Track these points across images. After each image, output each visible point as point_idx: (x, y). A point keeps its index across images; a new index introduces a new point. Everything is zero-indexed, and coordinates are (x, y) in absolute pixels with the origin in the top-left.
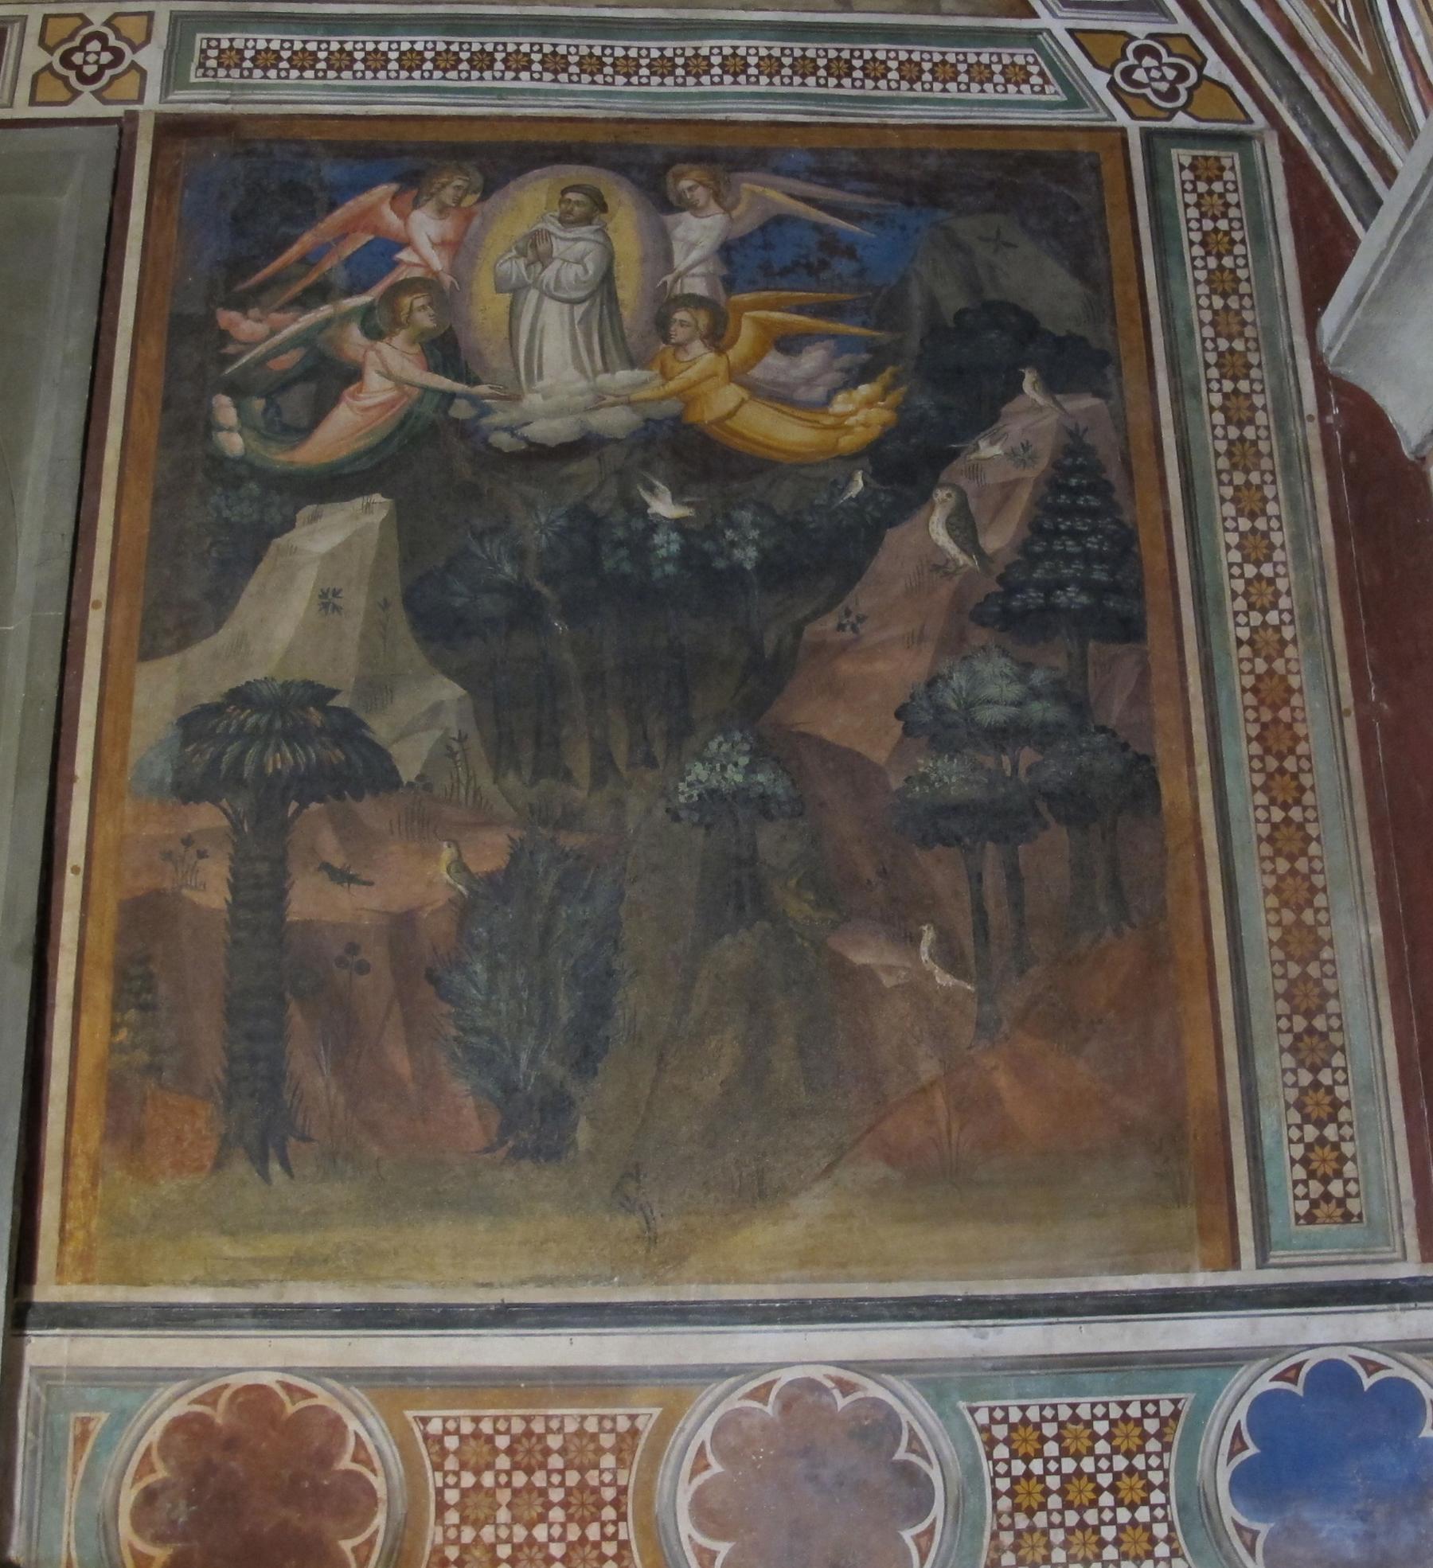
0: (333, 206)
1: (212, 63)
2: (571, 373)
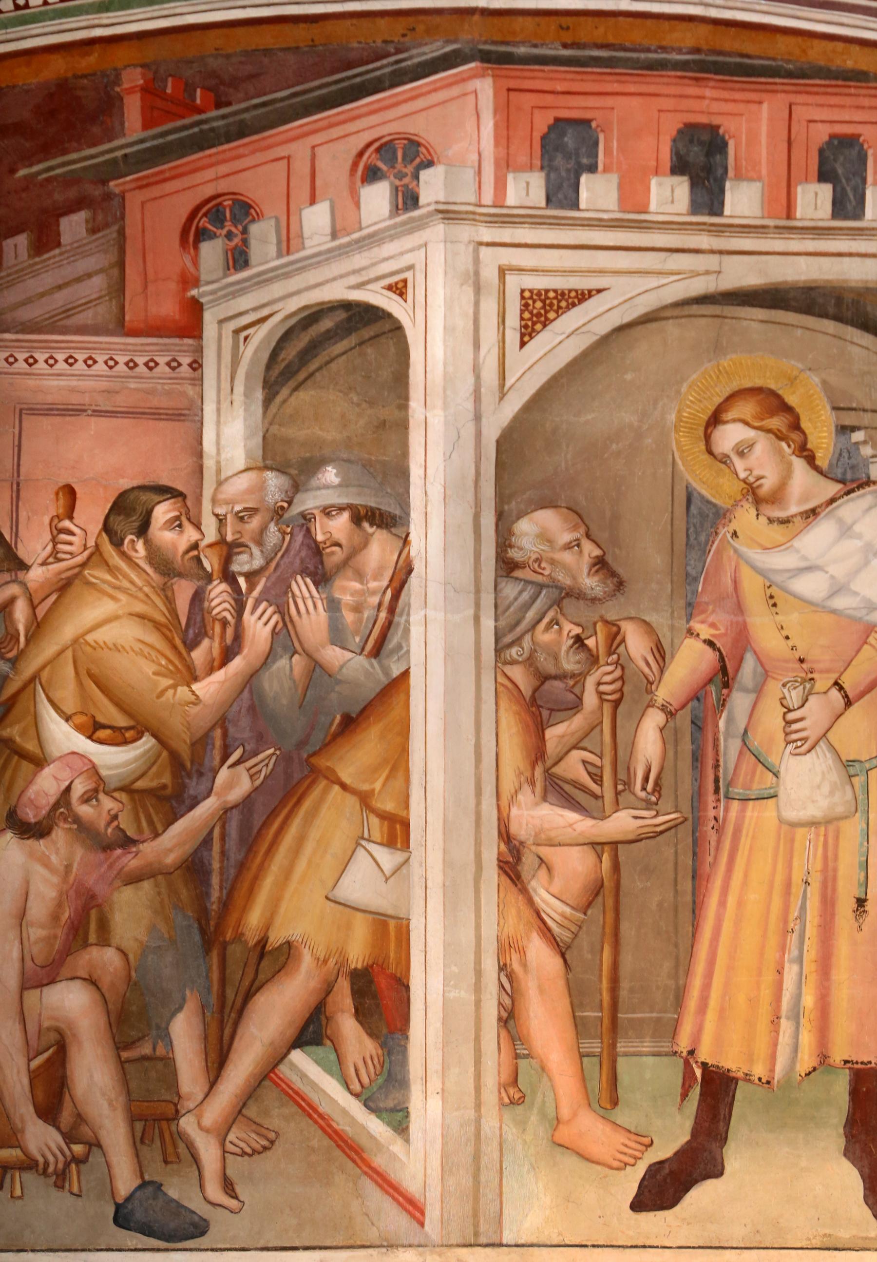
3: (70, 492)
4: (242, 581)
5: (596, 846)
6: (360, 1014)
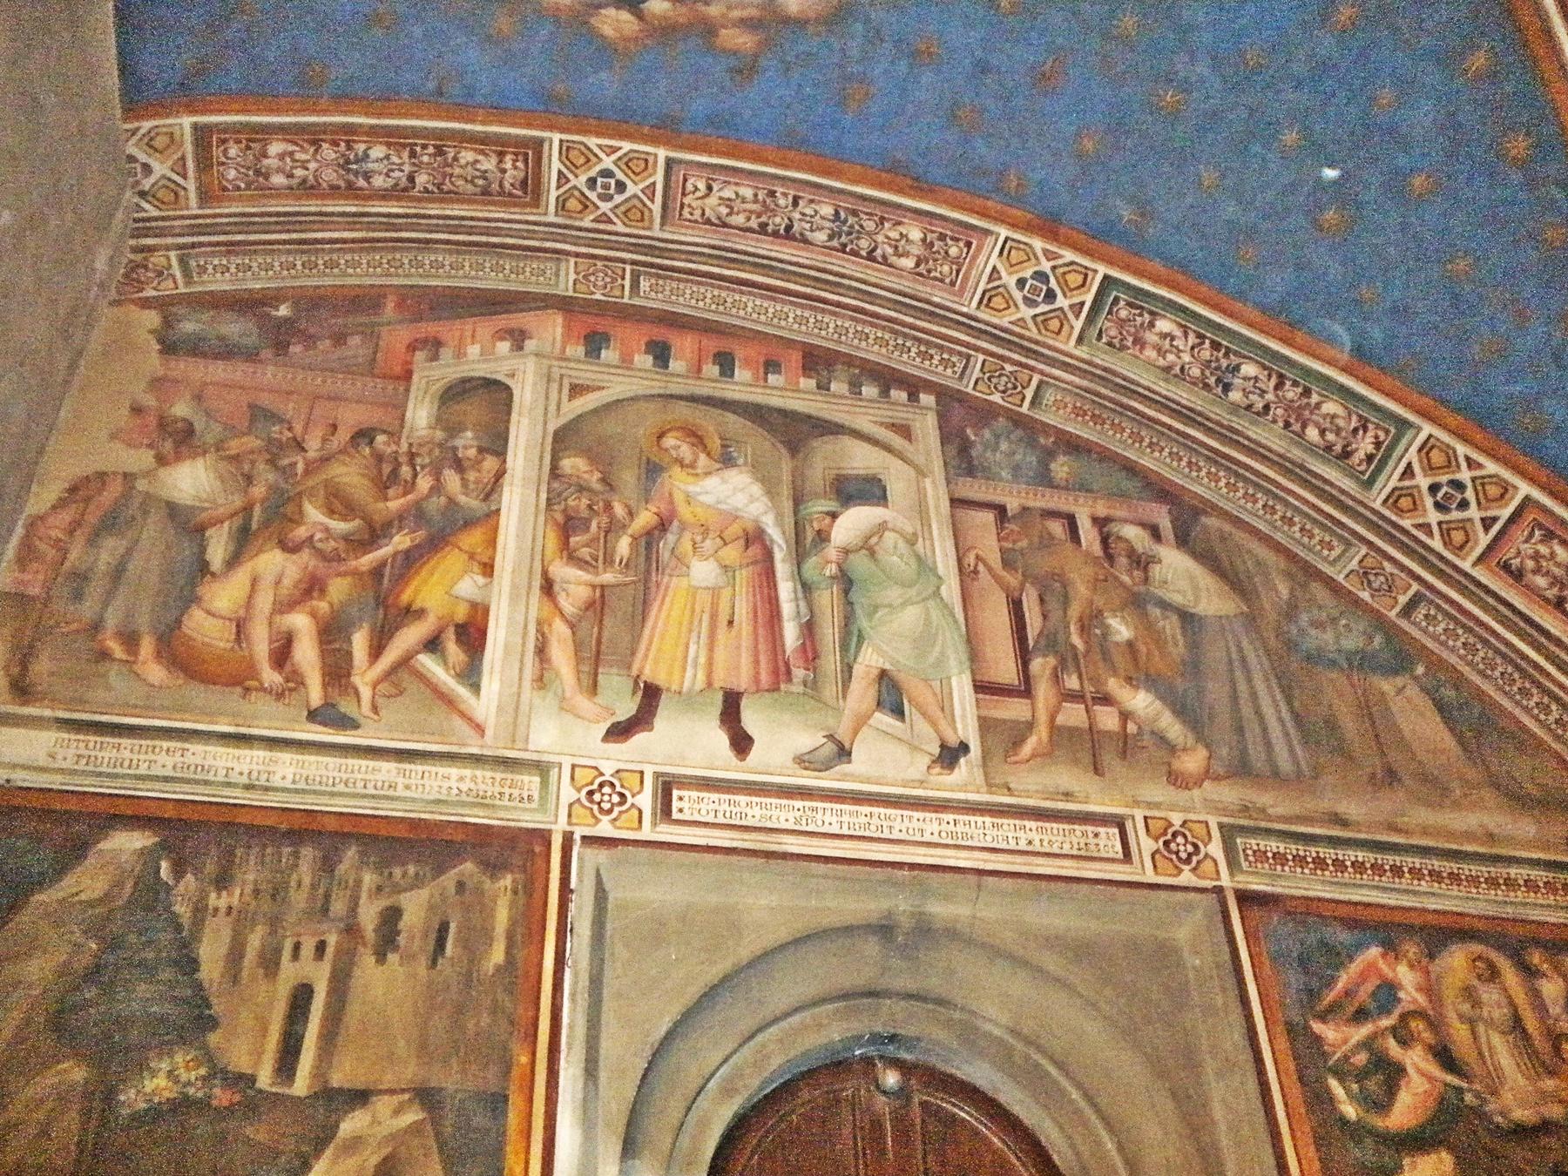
0: (1351, 959)
1: (1251, 858)
2: (1522, 1081)
3: (335, 427)
4: (418, 468)
5: (594, 587)
6: (459, 641)
